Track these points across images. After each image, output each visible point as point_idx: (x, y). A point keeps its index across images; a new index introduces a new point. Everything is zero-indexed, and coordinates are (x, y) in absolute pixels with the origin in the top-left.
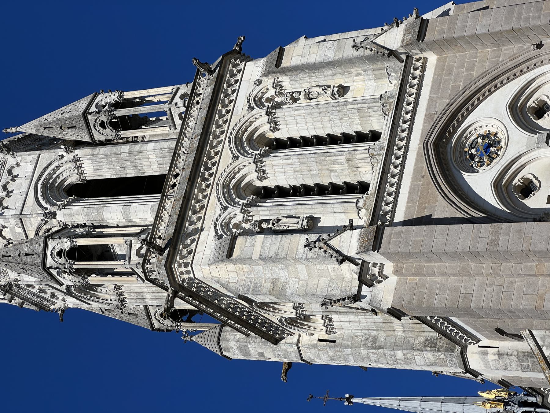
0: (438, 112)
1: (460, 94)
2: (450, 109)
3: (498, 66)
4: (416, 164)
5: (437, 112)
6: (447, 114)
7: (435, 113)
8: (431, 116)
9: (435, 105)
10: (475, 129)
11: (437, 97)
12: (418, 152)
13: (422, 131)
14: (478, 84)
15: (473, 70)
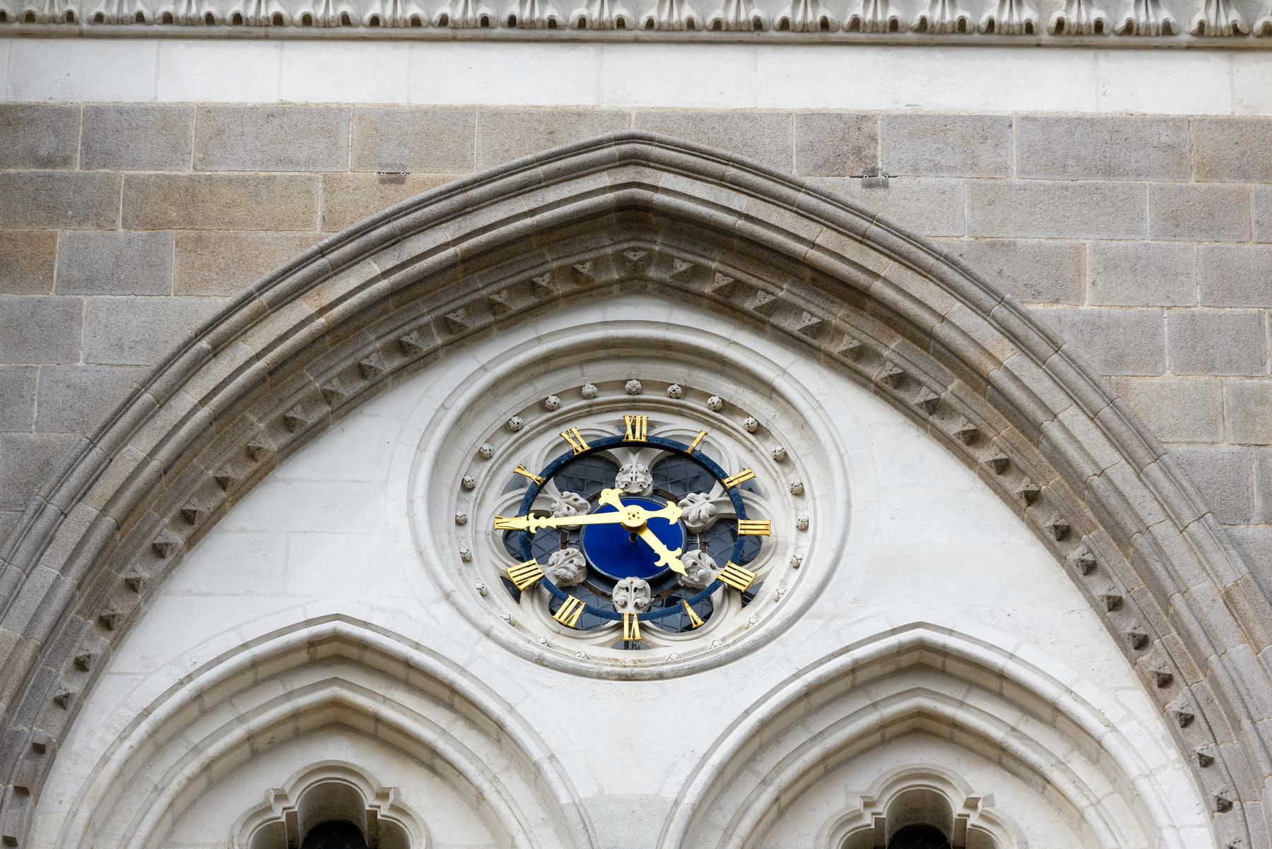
0: (880, 193)
1: (998, 310)
2: (889, 268)
3: (1187, 516)
4: (495, 117)
5: (885, 185)
6: (853, 250)
7: (873, 172)
8: (858, 151)
9: (937, 168)
10: (782, 459)
11: (1002, 168)
12: (580, 115)
13: (744, 116)
14: (1072, 416)
15: (1184, 367)
